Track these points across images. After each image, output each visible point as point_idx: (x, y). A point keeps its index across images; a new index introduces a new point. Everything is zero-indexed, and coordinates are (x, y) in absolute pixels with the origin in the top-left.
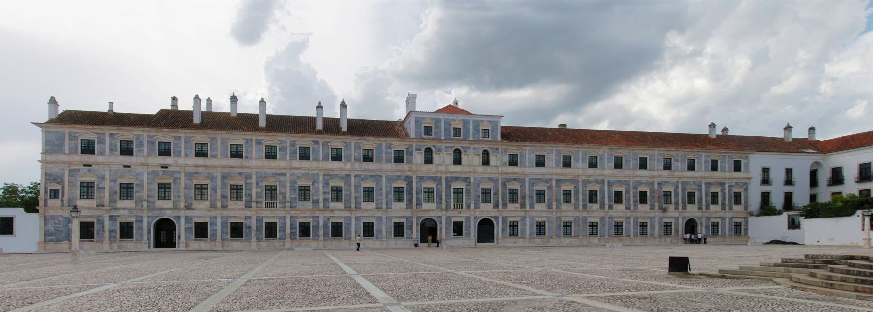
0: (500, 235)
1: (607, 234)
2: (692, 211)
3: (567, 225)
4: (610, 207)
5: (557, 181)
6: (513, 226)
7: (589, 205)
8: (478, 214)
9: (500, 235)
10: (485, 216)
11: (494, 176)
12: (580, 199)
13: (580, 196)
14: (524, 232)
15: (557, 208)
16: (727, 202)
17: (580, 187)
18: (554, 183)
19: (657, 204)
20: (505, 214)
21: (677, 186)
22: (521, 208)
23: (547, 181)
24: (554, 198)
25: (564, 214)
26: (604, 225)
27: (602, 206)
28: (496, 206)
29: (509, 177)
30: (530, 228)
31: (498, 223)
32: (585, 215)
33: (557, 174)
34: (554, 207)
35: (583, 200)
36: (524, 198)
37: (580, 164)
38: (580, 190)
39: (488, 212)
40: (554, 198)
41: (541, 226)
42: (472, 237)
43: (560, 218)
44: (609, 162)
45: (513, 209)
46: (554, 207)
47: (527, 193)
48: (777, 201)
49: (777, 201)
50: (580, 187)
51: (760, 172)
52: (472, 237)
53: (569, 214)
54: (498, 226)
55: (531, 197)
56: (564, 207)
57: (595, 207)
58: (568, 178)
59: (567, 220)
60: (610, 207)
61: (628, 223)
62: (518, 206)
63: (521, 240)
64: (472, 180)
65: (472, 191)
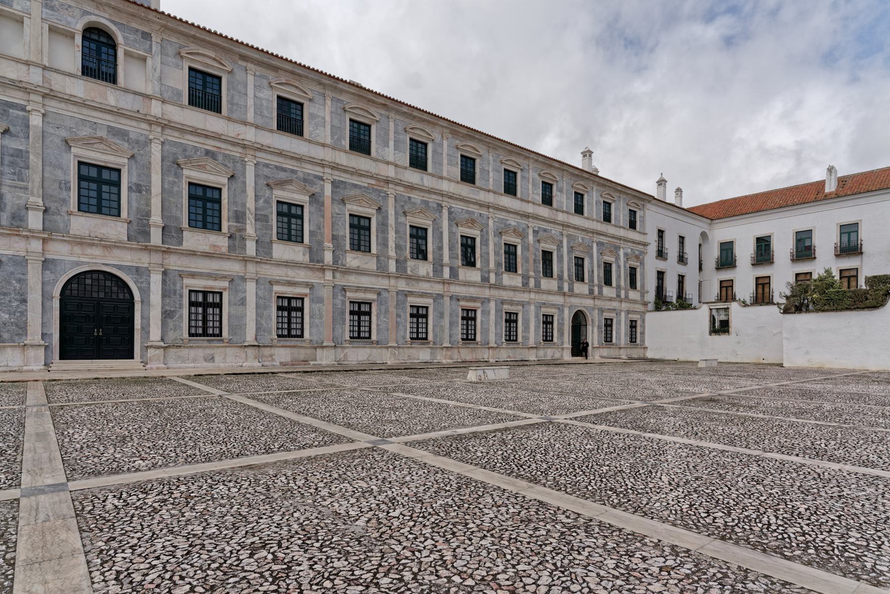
0: (155, 334)
1: (447, 338)
2: (581, 297)
3: (360, 311)
4: (454, 273)
5: (335, 184)
6: (289, 309)
7: (411, 263)
8: (59, 250)
9: (155, 334)
10: (95, 259)
11: (135, 129)
12: (392, 244)
13: (392, 235)
14: (238, 327)
15: (335, 260)
16: (622, 283)
17: (391, 212)
18: (328, 189)
19: (532, 274)
20: (175, 263)
21: (561, 242)
22: (231, 248)
23: (307, 180)
24: (327, 232)
25: (353, 280)
26: (442, 315)
27: (438, 266)
28: (139, 232)
29: (190, 141)
30: (259, 315)
31: (145, 292)
32: (402, 285)
33: (335, 167)
34: (328, 257)
35: (398, 247)
36: (239, 217)
37: (390, 154)
38: (391, 221)
39: (108, 245)
40: (327, 232)
41: (290, 309)
42: (34, 335)
43: (344, 290)
44: (450, 163)
45: (207, 249)
46: (328, 257)
47: (251, 204)
48: (671, 290)
49: (671, 290)
50: (391, 212)
51: (656, 232)
52: (34, 335)
53: (365, 281)
54: (145, 301)
55: (261, 218)
56: (353, 260)
57: (424, 268)
58: (364, 182)
59: (360, 296)
60: (454, 273)
61: (486, 313)
62: (220, 242)
63: (230, 351)
64: (36, 120)
65: (34, 160)
